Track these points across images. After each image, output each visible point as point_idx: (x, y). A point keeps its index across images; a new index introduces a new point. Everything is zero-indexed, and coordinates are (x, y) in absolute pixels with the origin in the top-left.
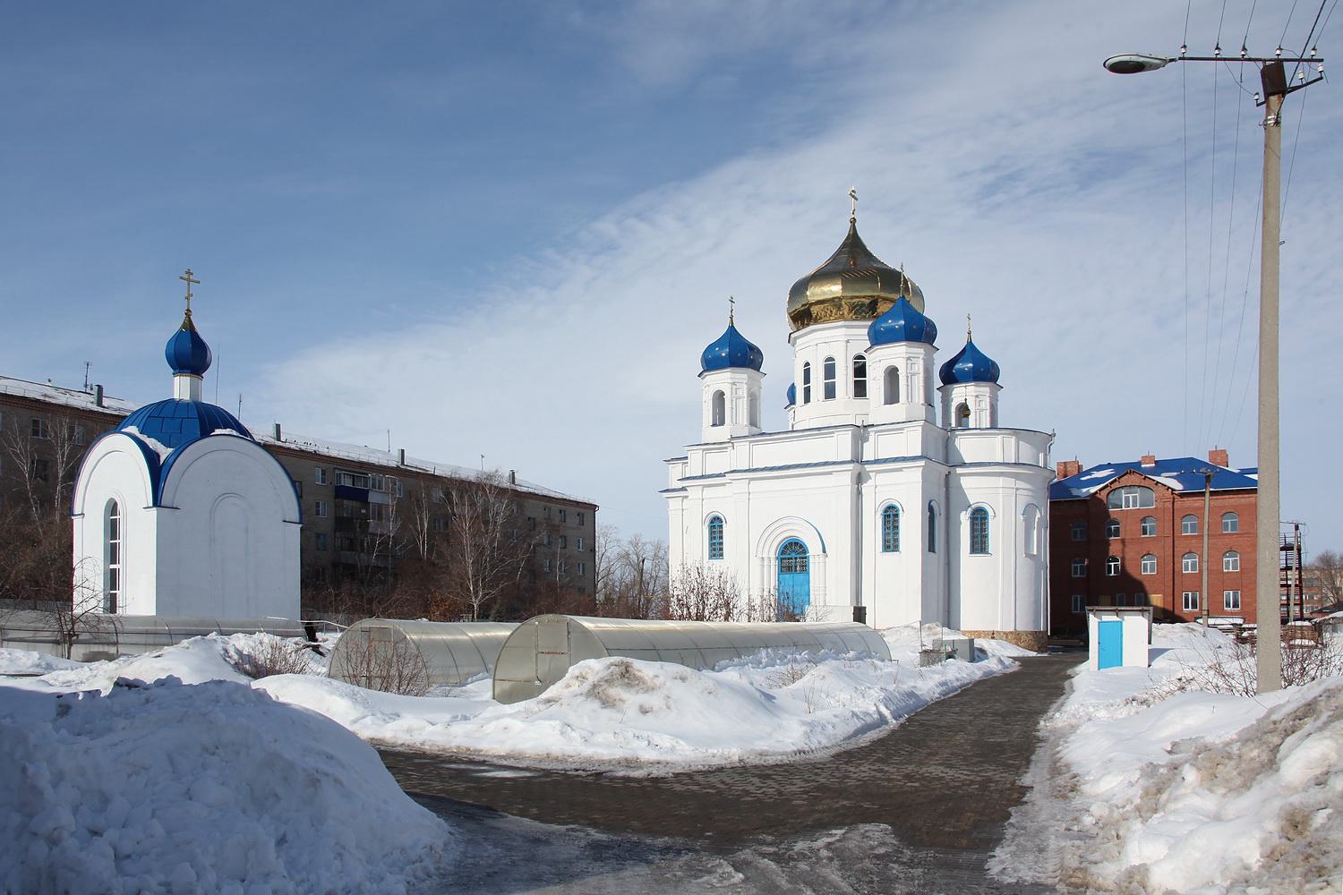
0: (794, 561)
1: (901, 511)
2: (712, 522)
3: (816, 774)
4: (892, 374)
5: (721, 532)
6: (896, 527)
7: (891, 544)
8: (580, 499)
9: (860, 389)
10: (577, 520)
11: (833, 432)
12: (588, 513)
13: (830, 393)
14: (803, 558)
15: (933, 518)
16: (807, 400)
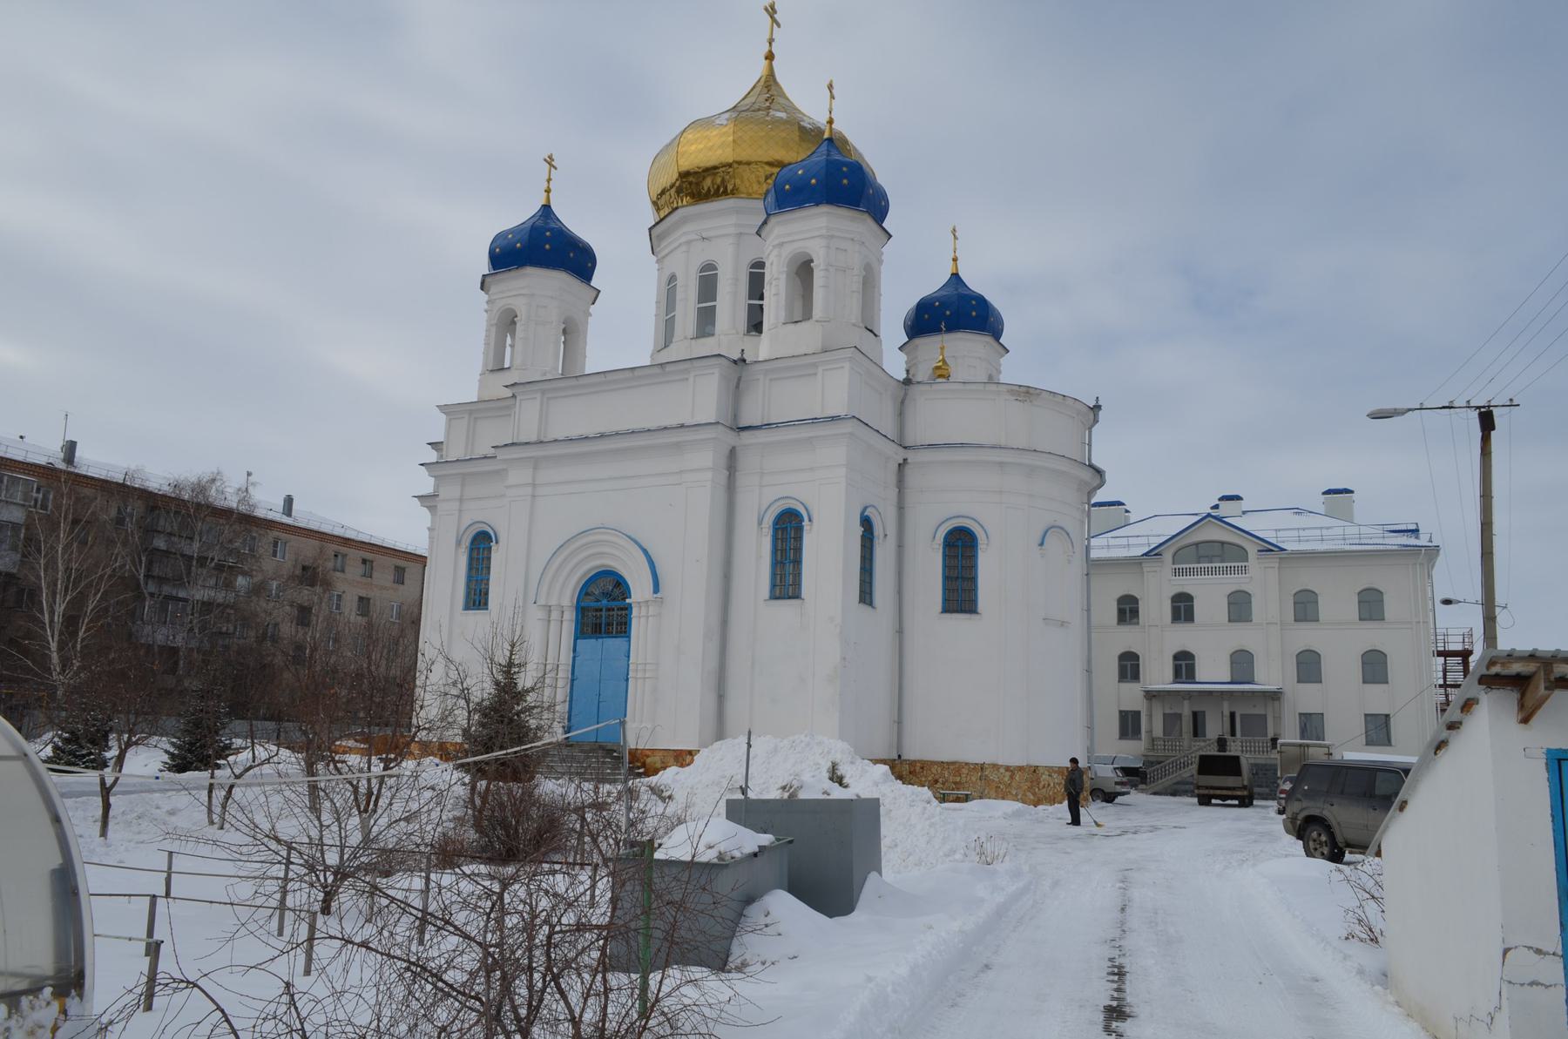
1: (806, 523)
4: (804, 270)
6: (798, 550)
8: (401, 546)
10: (360, 569)
12: (412, 569)
13: (706, 319)
15: (871, 540)
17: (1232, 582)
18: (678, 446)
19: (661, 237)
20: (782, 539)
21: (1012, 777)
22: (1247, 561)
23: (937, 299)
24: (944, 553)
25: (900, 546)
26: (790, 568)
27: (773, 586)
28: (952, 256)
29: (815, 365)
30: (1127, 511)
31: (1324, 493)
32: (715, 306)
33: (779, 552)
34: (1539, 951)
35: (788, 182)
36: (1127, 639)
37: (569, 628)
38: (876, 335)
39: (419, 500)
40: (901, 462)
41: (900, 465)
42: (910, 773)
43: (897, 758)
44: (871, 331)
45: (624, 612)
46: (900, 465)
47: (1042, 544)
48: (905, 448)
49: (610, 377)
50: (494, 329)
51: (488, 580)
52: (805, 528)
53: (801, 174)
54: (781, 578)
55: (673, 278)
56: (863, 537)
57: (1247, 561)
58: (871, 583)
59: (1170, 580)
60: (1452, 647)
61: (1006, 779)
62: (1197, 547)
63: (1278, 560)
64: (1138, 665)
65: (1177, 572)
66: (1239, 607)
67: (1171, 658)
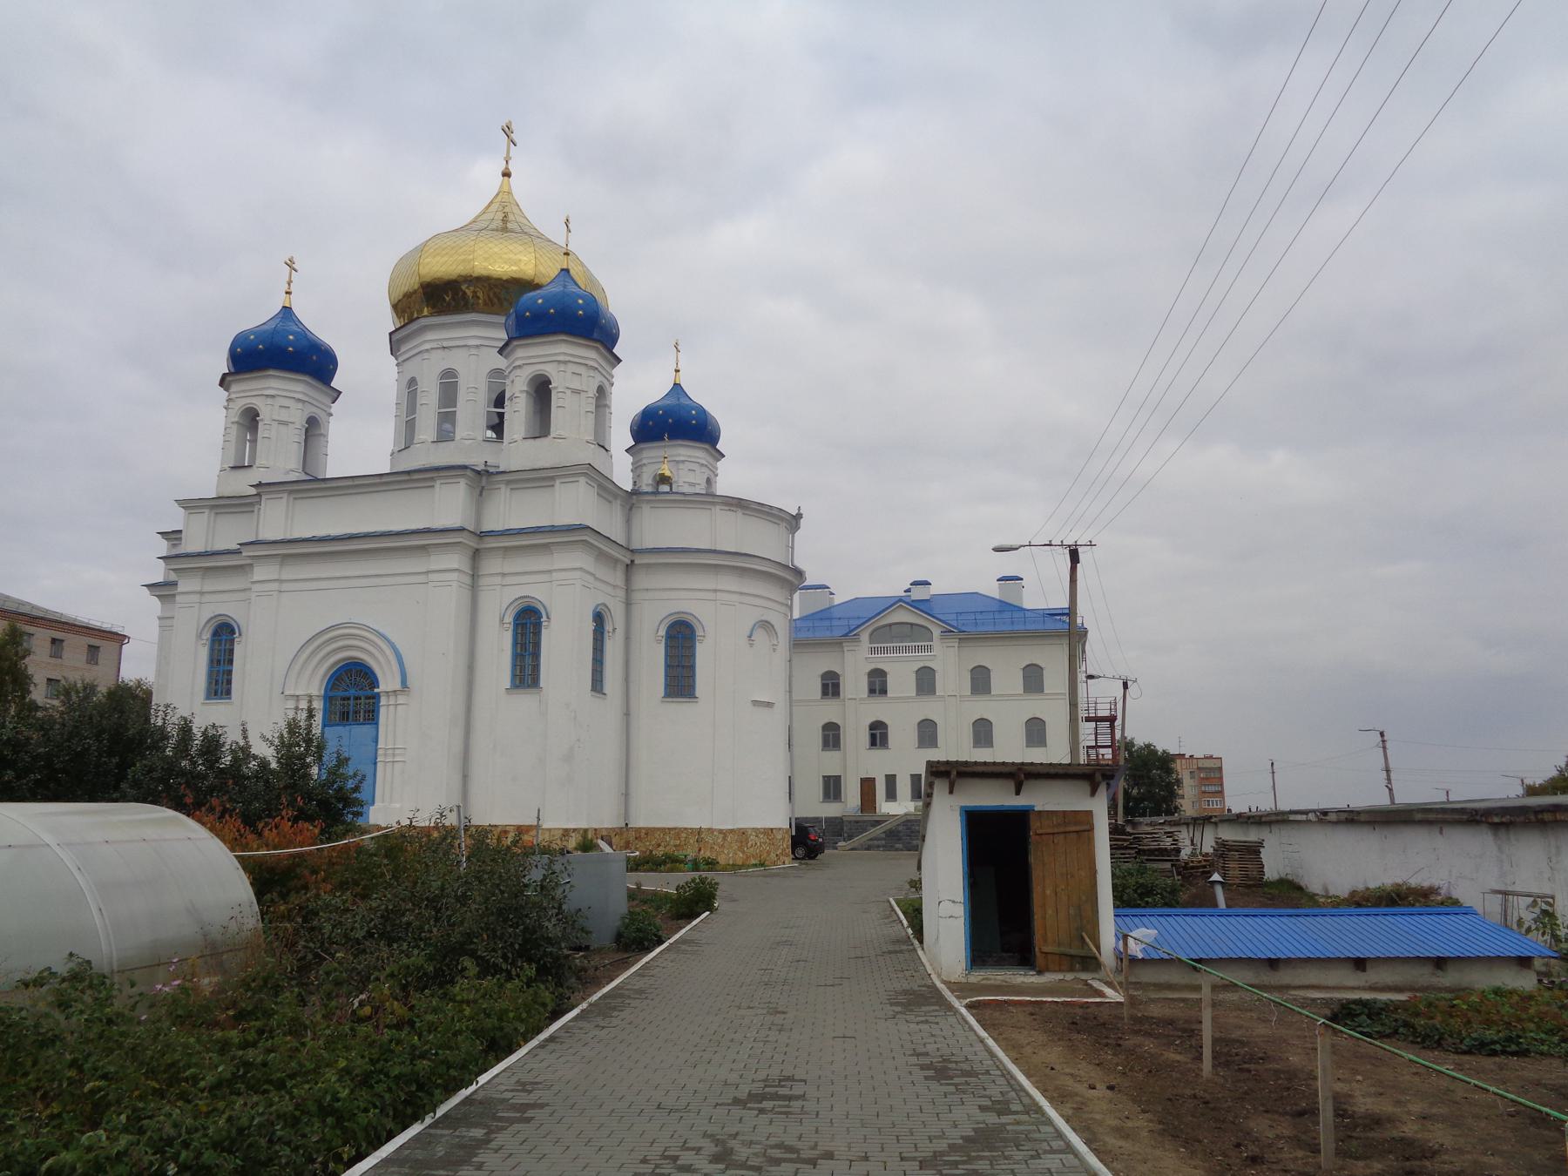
1: (544, 618)
4: (541, 390)
5: (231, 651)
6: (537, 645)
7: (526, 671)
11: (432, 479)
12: (106, 647)
14: (368, 698)
15: (602, 633)
18: (423, 548)
20: (522, 635)
21: (724, 839)
23: (659, 408)
24: (666, 644)
25: (627, 638)
26: (529, 660)
27: (514, 676)
29: (553, 478)
31: (998, 580)
32: (455, 412)
33: (519, 645)
34: (954, 902)
35: (528, 310)
36: (829, 711)
38: (607, 450)
39: (149, 589)
40: (629, 562)
41: (627, 565)
42: (636, 838)
43: (624, 826)
44: (603, 447)
45: (371, 701)
46: (627, 565)
47: (750, 637)
48: (632, 551)
49: (357, 482)
50: (234, 429)
51: (230, 672)
52: (544, 624)
53: (541, 303)
54: (521, 669)
55: (412, 382)
56: (595, 631)
59: (866, 658)
60: (1100, 714)
61: (719, 841)
62: (890, 629)
63: (957, 640)
64: (839, 734)
65: (873, 651)
66: (926, 681)
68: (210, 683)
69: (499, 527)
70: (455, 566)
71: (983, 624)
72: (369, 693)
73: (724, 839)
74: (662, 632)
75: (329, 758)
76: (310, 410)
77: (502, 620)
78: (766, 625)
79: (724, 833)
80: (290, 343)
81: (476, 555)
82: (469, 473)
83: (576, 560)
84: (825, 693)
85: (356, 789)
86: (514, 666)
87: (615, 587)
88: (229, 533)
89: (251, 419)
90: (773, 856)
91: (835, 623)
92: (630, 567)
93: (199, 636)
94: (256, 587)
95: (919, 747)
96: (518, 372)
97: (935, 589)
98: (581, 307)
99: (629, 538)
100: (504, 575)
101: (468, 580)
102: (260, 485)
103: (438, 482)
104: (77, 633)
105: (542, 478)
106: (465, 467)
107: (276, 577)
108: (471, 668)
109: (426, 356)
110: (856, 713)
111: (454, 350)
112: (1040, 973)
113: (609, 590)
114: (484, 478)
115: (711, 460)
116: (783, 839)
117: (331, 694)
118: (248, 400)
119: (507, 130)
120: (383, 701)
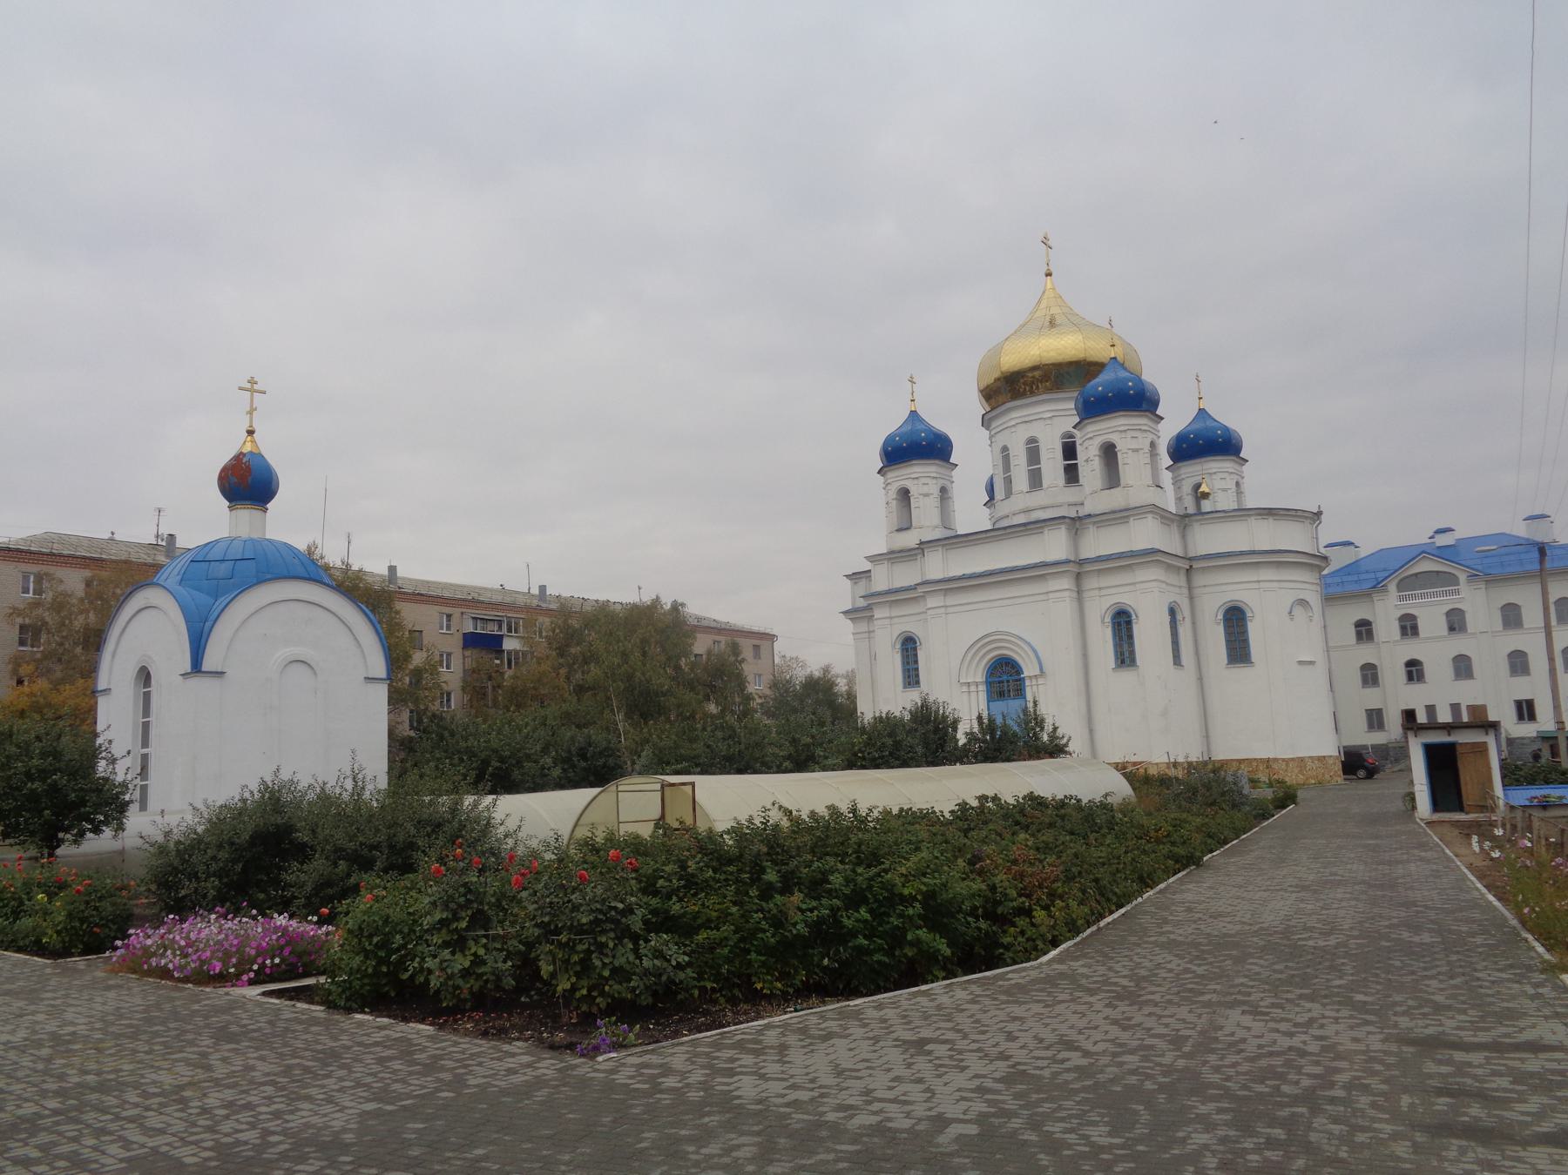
0: (1005, 684)
1: (1134, 617)
2: (903, 644)
3: (1011, 1037)
4: (1109, 453)
5: (916, 655)
6: (1130, 637)
7: (1125, 656)
8: (755, 629)
9: (1072, 474)
12: (764, 644)
13: (1036, 480)
14: (1017, 681)
16: (1009, 493)
17: (1448, 603)
19: (991, 420)
21: (1287, 765)
22: (1458, 585)
26: (1125, 647)
27: (1117, 658)
28: (1197, 396)
29: (1127, 517)
30: (1357, 547)
31: (1524, 520)
36: (1366, 654)
37: (983, 696)
48: (1190, 559)
51: (917, 669)
57: (1458, 585)
58: (1178, 651)
65: (1401, 598)
66: (1456, 622)
67: (1403, 666)
68: (904, 678)
69: (1092, 555)
70: (1067, 587)
71: (1510, 565)
72: (1016, 677)
73: (1287, 765)
74: (1220, 616)
75: (1048, 728)
76: (941, 483)
77: (1103, 622)
78: (1303, 603)
79: (1286, 761)
80: (923, 439)
81: (1078, 577)
82: (1067, 520)
83: (1150, 575)
84: (1359, 636)
85: (1066, 745)
86: (1116, 652)
87: (1180, 587)
88: (905, 576)
89: (905, 494)
90: (1327, 777)
91: (1363, 576)
92: (1189, 571)
93: (894, 646)
94: (930, 612)
95: (1456, 680)
96: (1091, 442)
97: (1462, 532)
98: (1130, 388)
99: (1186, 552)
100: (1100, 589)
101: (1075, 595)
102: (921, 543)
103: (1046, 529)
104: (746, 637)
105: (1120, 516)
106: (1064, 517)
107: (942, 604)
108: (1085, 655)
109: (1013, 429)
110: (1391, 652)
111: (1035, 423)
112: (1467, 813)
113: (1177, 590)
114: (1078, 523)
115: (1237, 466)
116: (1335, 764)
117: (989, 680)
118: (902, 483)
119: (1045, 242)
120: (1027, 683)
